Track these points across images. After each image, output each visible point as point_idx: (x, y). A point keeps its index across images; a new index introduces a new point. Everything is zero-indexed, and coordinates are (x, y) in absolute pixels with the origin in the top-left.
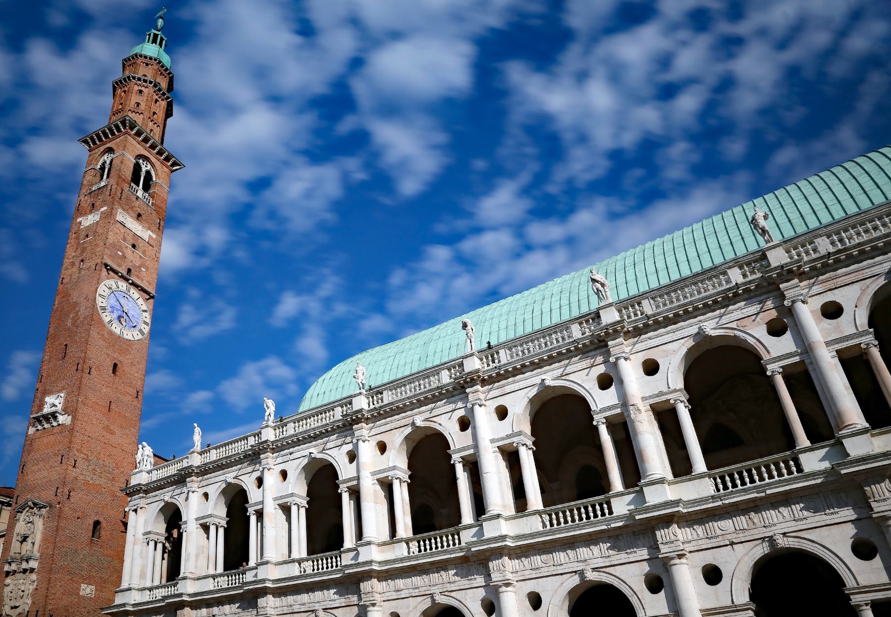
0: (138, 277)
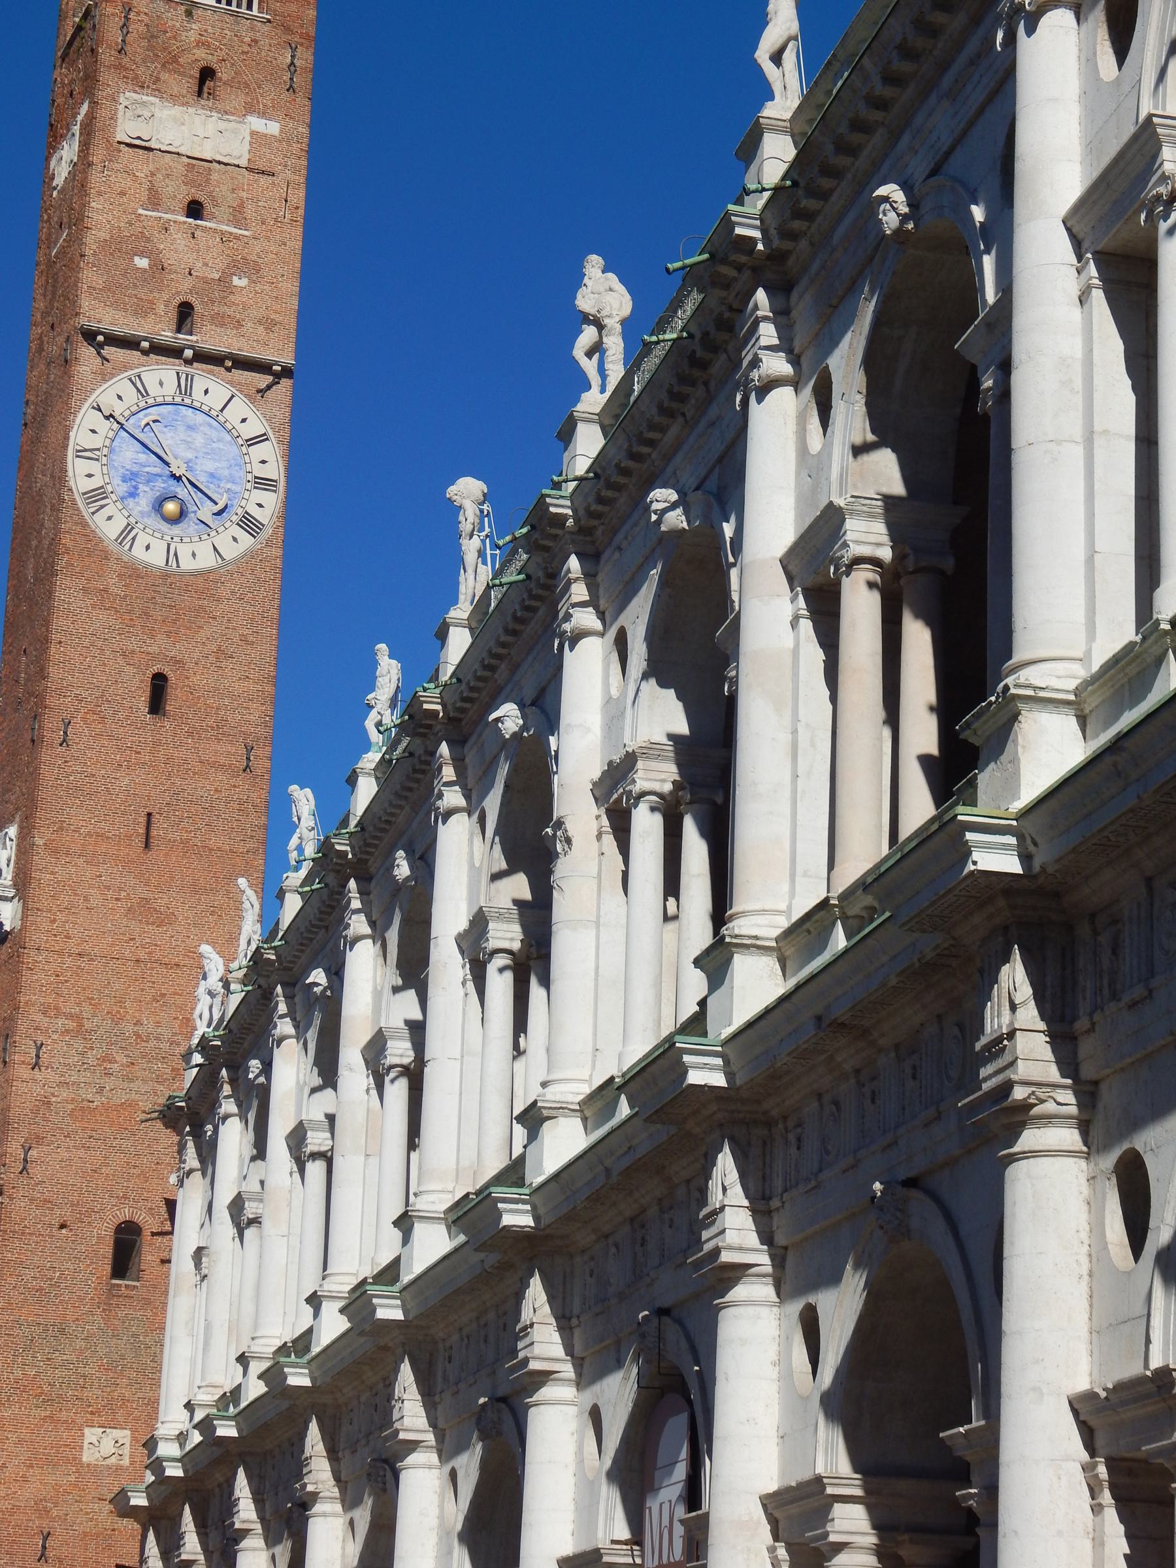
0: (220, 320)
